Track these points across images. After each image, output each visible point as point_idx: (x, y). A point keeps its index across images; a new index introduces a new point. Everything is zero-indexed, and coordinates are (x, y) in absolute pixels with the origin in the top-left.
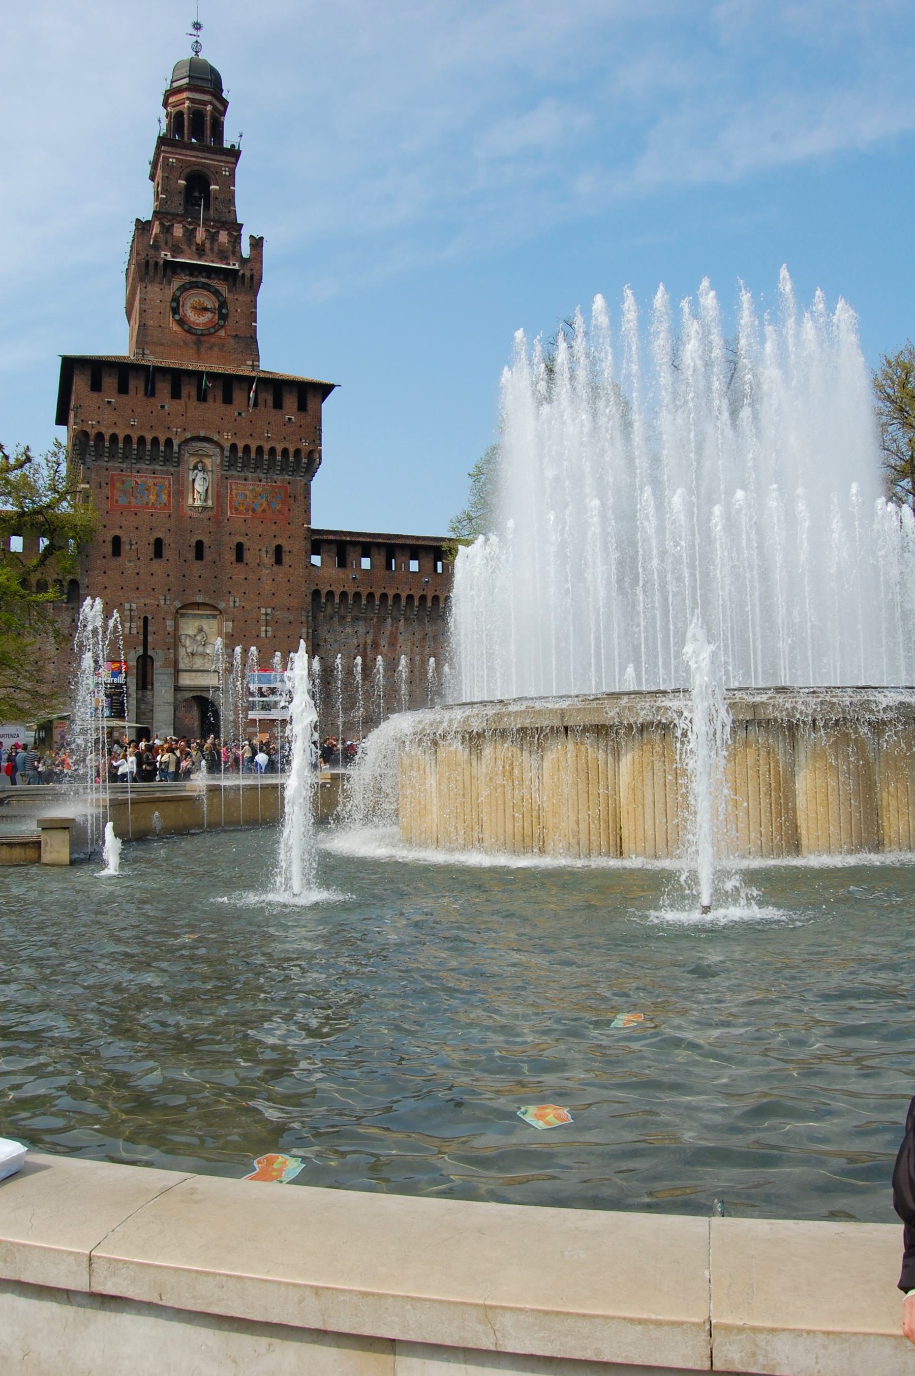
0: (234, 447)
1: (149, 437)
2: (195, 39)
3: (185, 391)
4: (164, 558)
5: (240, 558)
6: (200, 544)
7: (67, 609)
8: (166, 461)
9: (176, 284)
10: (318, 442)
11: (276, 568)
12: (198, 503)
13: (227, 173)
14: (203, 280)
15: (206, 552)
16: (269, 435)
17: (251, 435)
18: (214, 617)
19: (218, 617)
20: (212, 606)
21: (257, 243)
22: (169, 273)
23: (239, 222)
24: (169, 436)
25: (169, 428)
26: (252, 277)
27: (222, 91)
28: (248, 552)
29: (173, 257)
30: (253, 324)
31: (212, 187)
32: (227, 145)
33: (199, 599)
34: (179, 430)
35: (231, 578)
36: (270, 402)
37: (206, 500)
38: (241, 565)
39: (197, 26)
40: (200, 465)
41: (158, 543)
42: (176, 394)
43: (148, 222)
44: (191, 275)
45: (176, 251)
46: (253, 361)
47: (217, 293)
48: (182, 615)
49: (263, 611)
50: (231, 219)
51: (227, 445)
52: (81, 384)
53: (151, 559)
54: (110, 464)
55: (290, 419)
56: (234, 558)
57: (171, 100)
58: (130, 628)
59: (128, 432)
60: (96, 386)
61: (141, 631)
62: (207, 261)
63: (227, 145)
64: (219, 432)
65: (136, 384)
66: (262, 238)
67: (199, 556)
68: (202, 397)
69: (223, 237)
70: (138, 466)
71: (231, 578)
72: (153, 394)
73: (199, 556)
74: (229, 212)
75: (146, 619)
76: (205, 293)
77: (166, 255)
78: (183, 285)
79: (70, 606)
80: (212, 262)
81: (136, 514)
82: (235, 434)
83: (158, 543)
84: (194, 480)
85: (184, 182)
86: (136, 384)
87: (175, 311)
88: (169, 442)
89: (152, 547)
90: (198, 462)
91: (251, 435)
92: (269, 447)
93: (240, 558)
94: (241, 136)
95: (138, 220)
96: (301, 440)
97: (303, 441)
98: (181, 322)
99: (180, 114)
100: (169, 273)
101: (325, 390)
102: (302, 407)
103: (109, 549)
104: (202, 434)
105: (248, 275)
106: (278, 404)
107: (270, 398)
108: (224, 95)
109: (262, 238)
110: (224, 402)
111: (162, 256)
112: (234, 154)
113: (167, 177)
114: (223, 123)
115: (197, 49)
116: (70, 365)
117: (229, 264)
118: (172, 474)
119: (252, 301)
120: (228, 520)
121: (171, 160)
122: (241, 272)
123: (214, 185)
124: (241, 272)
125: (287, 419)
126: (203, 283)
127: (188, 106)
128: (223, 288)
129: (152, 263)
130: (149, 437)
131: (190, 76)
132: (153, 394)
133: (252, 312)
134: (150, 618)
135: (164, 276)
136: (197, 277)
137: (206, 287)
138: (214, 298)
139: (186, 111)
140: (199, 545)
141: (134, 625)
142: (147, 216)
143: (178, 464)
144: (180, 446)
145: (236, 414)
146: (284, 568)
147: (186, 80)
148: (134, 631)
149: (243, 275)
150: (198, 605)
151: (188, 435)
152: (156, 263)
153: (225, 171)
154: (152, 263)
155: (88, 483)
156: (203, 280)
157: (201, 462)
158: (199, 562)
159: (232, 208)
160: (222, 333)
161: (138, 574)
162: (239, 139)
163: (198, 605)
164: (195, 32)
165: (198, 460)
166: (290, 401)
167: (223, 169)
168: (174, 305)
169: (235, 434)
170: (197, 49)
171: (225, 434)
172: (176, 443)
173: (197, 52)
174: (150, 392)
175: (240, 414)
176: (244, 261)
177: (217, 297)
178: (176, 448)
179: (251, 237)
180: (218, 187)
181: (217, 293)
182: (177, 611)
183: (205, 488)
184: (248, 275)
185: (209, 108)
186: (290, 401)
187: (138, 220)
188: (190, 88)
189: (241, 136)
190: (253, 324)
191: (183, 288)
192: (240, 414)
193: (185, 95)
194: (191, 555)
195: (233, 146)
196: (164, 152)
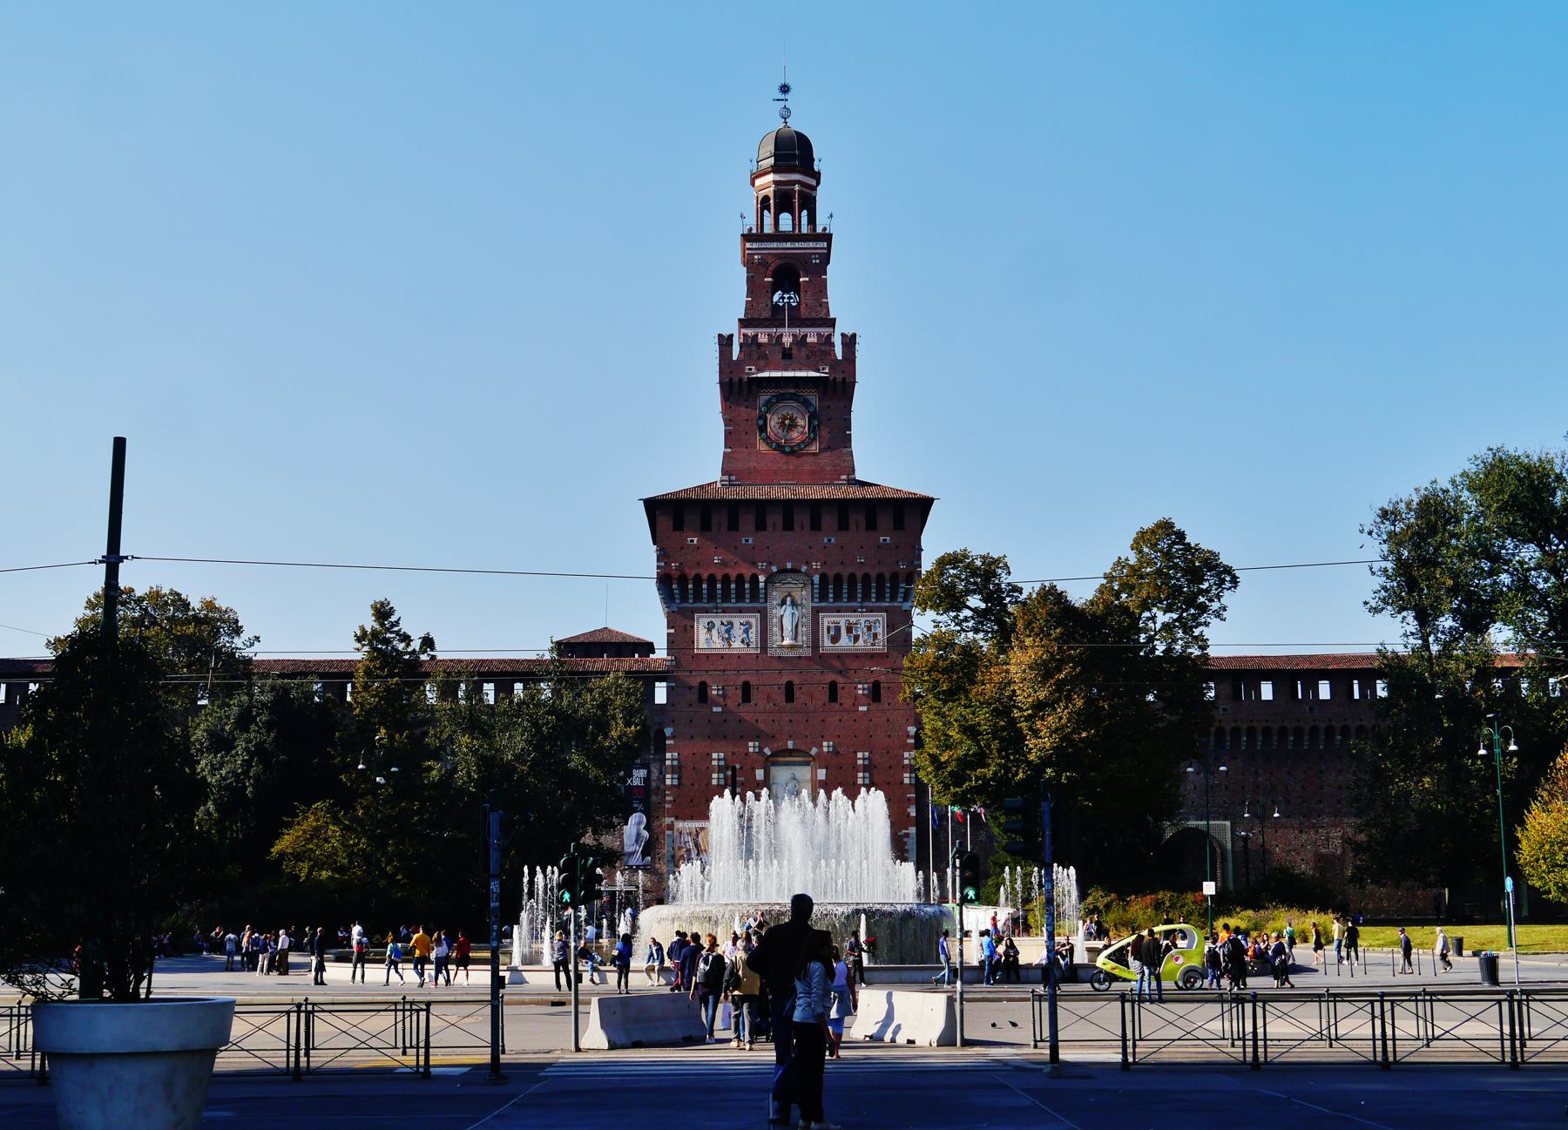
0: (823, 578)
1: (733, 574)
2: (782, 103)
3: (769, 522)
4: (753, 703)
5: (833, 697)
6: (790, 687)
7: (654, 760)
8: (755, 598)
9: (763, 399)
10: (916, 563)
11: (874, 706)
12: (787, 642)
13: (818, 261)
14: (792, 391)
15: (797, 694)
16: (862, 561)
17: (842, 563)
18: (807, 764)
19: (812, 763)
20: (804, 752)
21: (850, 342)
22: (755, 388)
23: (832, 316)
24: (754, 571)
25: (754, 563)
26: (844, 379)
27: (814, 160)
28: (843, 692)
29: (759, 370)
30: (848, 432)
31: (801, 280)
32: (819, 230)
33: (790, 744)
34: (765, 564)
35: (824, 720)
36: (863, 524)
37: (796, 639)
38: (837, 706)
39: (785, 89)
40: (789, 599)
41: (746, 687)
42: (761, 526)
43: (731, 336)
44: (777, 387)
45: (763, 360)
46: (848, 475)
47: (806, 403)
48: (775, 764)
49: (860, 755)
50: (822, 315)
51: (816, 579)
52: (665, 522)
53: (739, 705)
54: (696, 605)
55: (885, 540)
56: (825, 696)
57: (758, 182)
58: (718, 779)
59: (712, 571)
60: (678, 526)
61: (730, 781)
62: (794, 370)
63: (819, 230)
64: (807, 563)
65: (720, 519)
66: (854, 335)
67: (790, 697)
68: (788, 525)
69: (811, 339)
70: (724, 605)
71: (824, 720)
72: (737, 529)
73: (790, 697)
74: (821, 305)
75: (734, 769)
76: (794, 405)
77: (750, 369)
78: (769, 400)
79: (657, 757)
80: (800, 370)
81: (722, 657)
82: (825, 563)
83: (746, 687)
84: (782, 616)
85: (770, 279)
86: (720, 519)
87: (763, 429)
89: (740, 692)
90: (787, 596)
91: (842, 563)
92: (862, 573)
93: (833, 697)
94: (831, 216)
95: (720, 336)
96: (897, 562)
97: (900, 563)
98: (767, 440)
99: (766, 199)
100: (755, 388)
101: (924, 505)
102: (898, 525)
103: (694, 696)
104: (789, 566)
105: (839, 379)
106: (871, 526)
107: (862, 519)
108: (816, 170)
109: (854, 335)
110: (812, 529)
111: (747, 371)
112: (827, 238)
113: (752, 277)
114: (815, 197)
115: (786, 114)
116: (653, 506)
117: (818, 371)
118: (759, 612)
119: (845, 407)
120: (820, 657)
121: (756, 257)
122: (831, 378)
123: (804, 277)
124: (831, 378)
125: (881, 541)
126: (791, 393)
127: (774, 191)
128: (814, 399)
129: (736, 380)
130: (733, 574)
131: (775, 155)
132: (737, 529)
133: (845, 419)
134: (738, 766)
135: (750, 391)
136: (785, 388)
137: (793, 397)
138: (803, 409)
139: (771, 195)
140: (790, 687)
141: (722, 776)
142: (731, 328)
143: (766, 602)
144: (766, 582)
145: (826, 540)
146: (884, 705)
147: (771, 161)
148: (722, 782)
149: (835, 379)
150: (791, 752)
151: (774, 569)
152: (741, 379)
153: (816, 259)
154: (736, 380)
155: (673, 628)
156: (792, 391)
157: (789, 595)
158: (789, 704)
159: (824, 300)
161: (725, 721)
162: (829, 220)
163: (791, 752)
164: (782, 97)
165: (787, 594)
166: (884, 520)
167: (813, 257)
168: (761, 422)
169: (825, 563)
170: (786, 114)
171: (814, 564)
172: (762, 578)
173: (785, 119)
174: (733, 526)
175: (829, 540)
176: (835, 364)
177: (807, 408)
178: (762, 585)
179: (843, 335)
180: (807, 279)
181: (806, 403)
182: (767, 759)
183: (794, 624)
184: (839, 379)
185: (797, 187)
186: (884, 520)
187: (720, 336)
188: (775, 169)
189: (831, 216)
190: (848, 432)
191: (768, 404)
192: (829, 540)
193: (771, 177)
194: (780, 698)
195: (825, 229)
196: (748, 249)
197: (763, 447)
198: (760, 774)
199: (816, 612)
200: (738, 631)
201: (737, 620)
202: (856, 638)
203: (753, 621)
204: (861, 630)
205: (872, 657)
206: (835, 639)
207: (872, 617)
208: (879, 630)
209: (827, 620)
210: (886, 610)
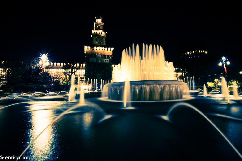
0: (103, 55)
88: (96, 55)
98: (97, 42)
160: (102, 43)
197: (96, 42)
198: (96, 74)
199: (102, 58)
200: (94, 60)
201: (94, 59)
202: (106, 61)
203: (96, 59)
204: (107, 61)
205: (108, 63)
206: (104, 61)
207: (108, 59)
208: (108, 61)
209: (103, 59)
210: (109, 59)
